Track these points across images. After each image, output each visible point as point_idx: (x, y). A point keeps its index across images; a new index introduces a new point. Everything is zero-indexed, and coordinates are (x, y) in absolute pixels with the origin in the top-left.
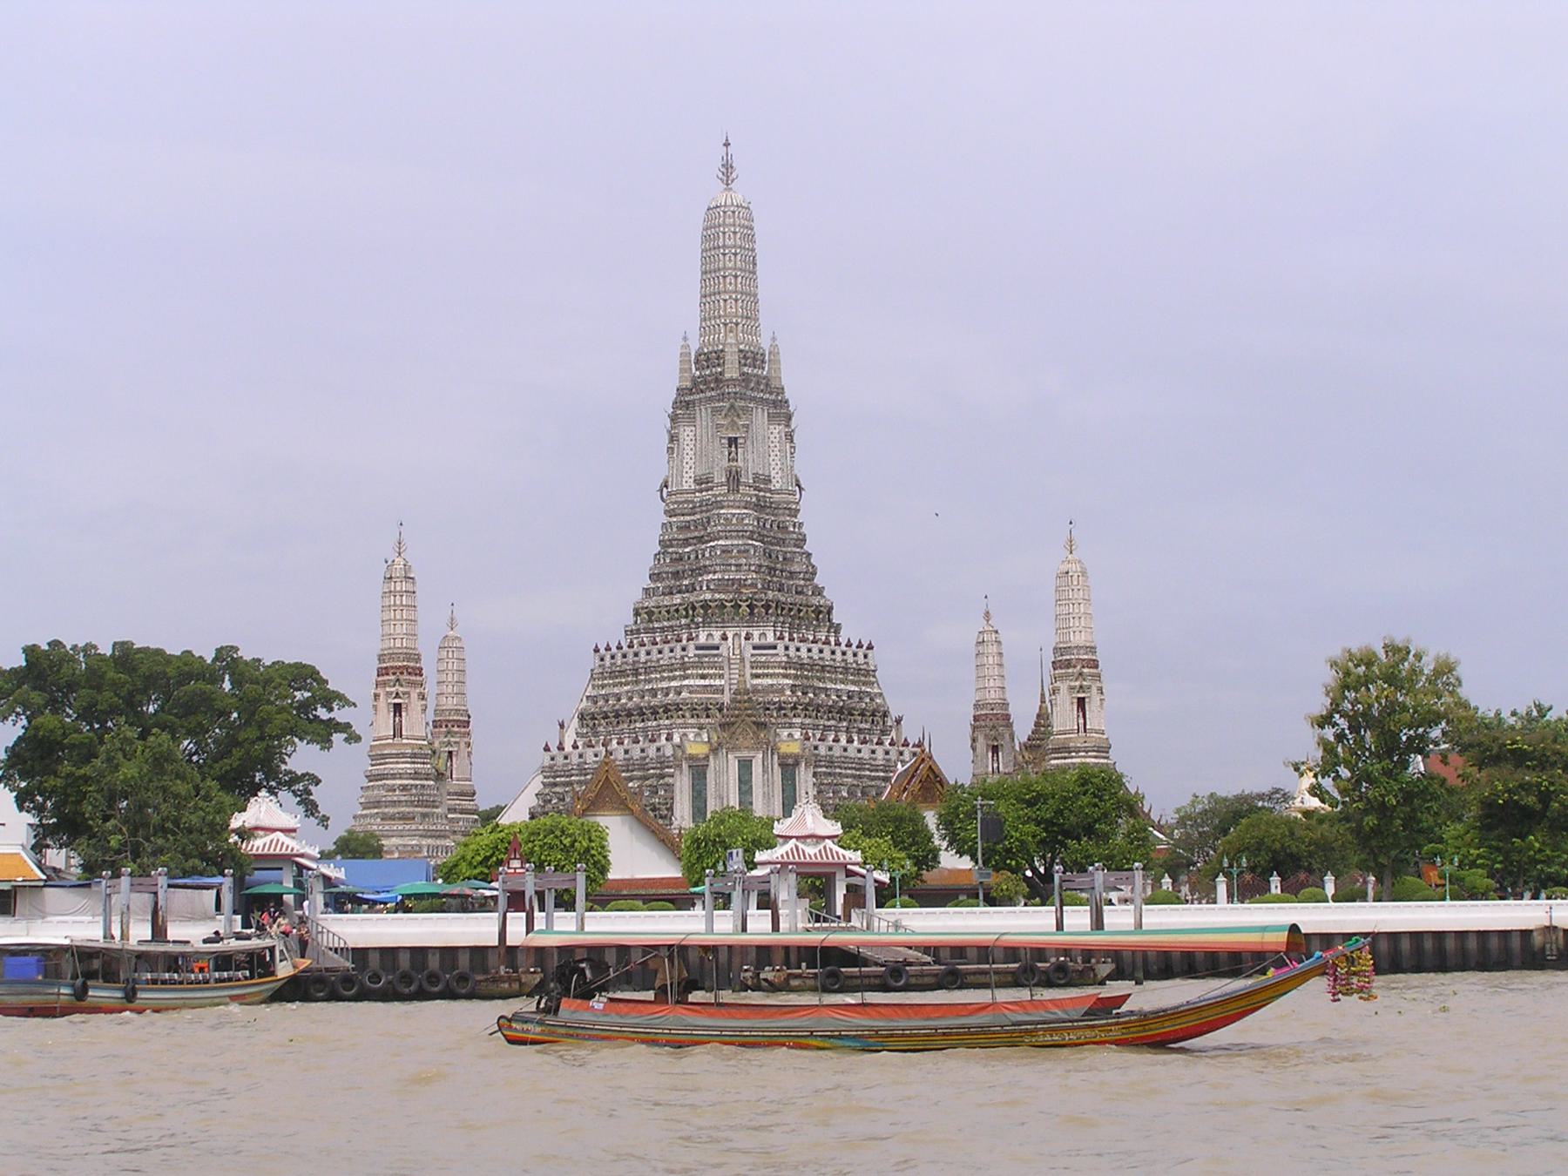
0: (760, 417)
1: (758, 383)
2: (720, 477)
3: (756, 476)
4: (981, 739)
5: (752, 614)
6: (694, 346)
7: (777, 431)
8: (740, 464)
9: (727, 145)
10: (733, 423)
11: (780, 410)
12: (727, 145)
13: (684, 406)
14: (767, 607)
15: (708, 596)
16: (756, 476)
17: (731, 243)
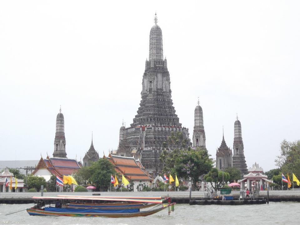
0: (160, 76)
1: (160, 68)
2: (148, 90)
3: (158, 89)
4: (235, 147)
5: (151, 121)
6: (148, 60)
7: (165, 78)
8: (152, 87)
9: (156, 14)
10: (151, 78)
11: (165, 73)
12: (156, 14)
13: (145, 74)
14: (154, 119)
15: (142, 117)
16: (158, 89)
17: (154, 37)
